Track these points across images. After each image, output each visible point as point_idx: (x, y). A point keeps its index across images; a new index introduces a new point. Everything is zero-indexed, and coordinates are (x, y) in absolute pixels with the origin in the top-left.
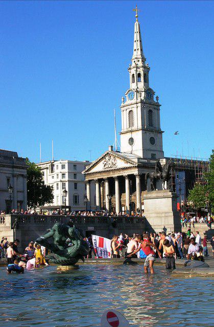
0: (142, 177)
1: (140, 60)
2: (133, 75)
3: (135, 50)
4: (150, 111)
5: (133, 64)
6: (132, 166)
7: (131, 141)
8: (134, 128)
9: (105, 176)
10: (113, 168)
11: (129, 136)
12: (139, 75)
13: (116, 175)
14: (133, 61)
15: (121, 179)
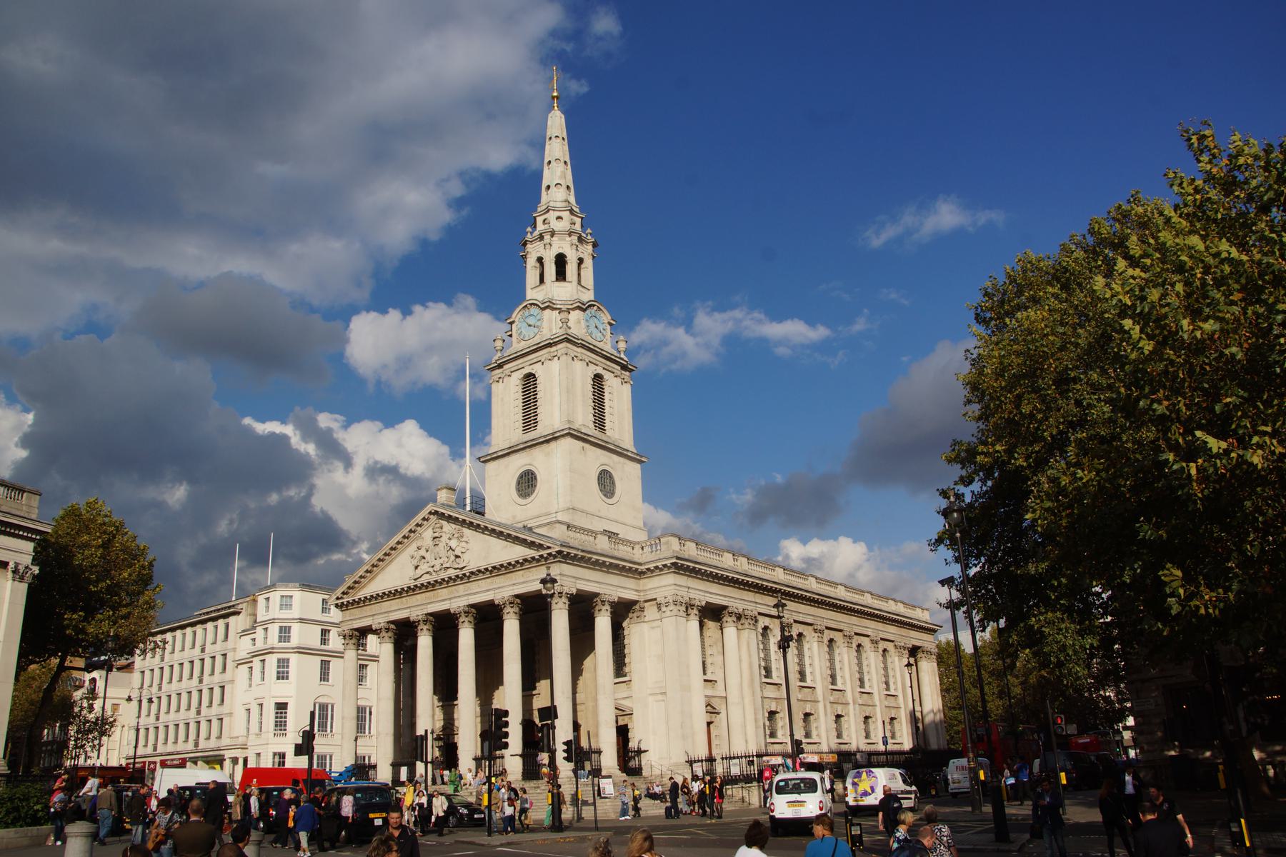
0: (582, 608)
1: (566, 215)
2: (540, 260)
3: (548, 187)
4: (598, 378)
5: (540, 227)
6: (530, 553)
7: (527, 482)
8: (543, 429)
9: (415, 608)
10: (452, 573)
11: (518, 464)
12: (561, 261)
13: (457, 600)
14: (539, 220)
15: (487, 618)
